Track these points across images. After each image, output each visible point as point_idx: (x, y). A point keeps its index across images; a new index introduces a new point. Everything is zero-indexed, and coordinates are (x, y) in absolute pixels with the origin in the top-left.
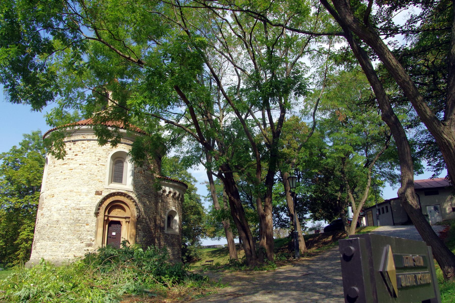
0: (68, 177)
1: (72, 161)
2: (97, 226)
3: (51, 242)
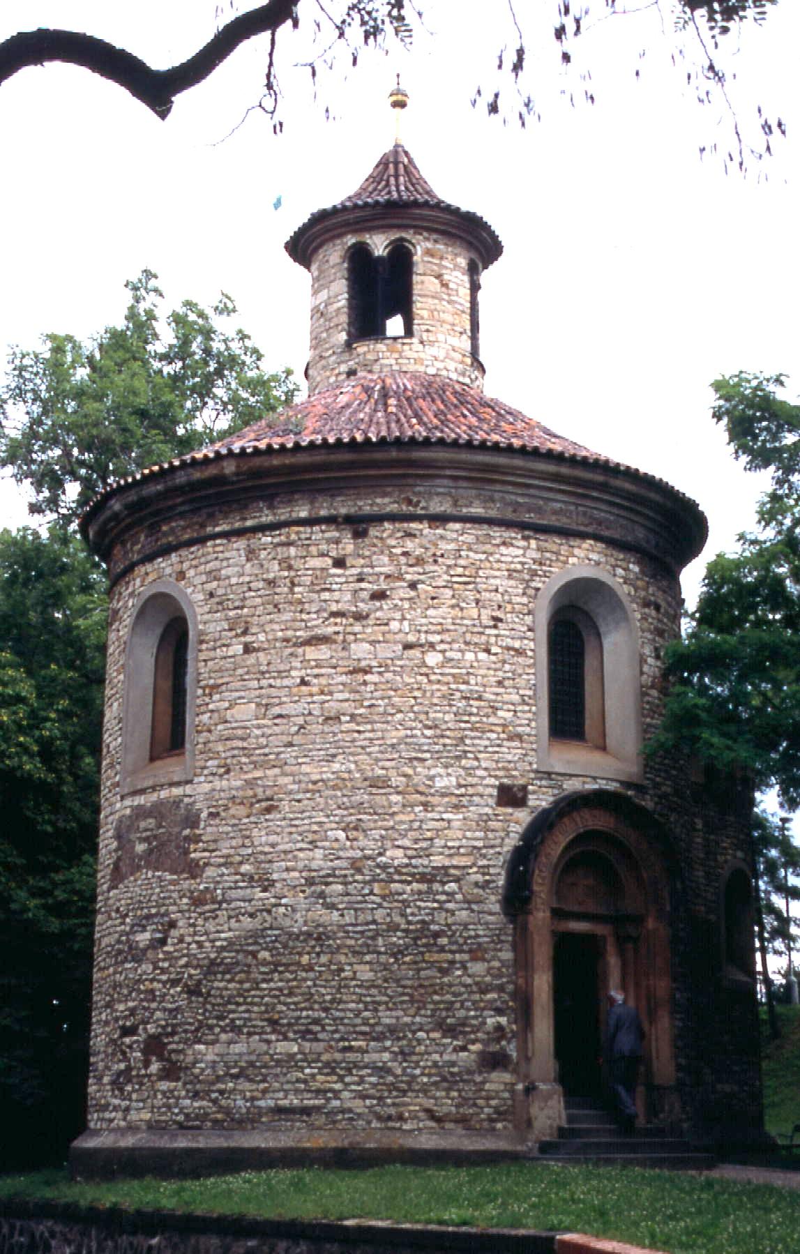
1: (357, 628)
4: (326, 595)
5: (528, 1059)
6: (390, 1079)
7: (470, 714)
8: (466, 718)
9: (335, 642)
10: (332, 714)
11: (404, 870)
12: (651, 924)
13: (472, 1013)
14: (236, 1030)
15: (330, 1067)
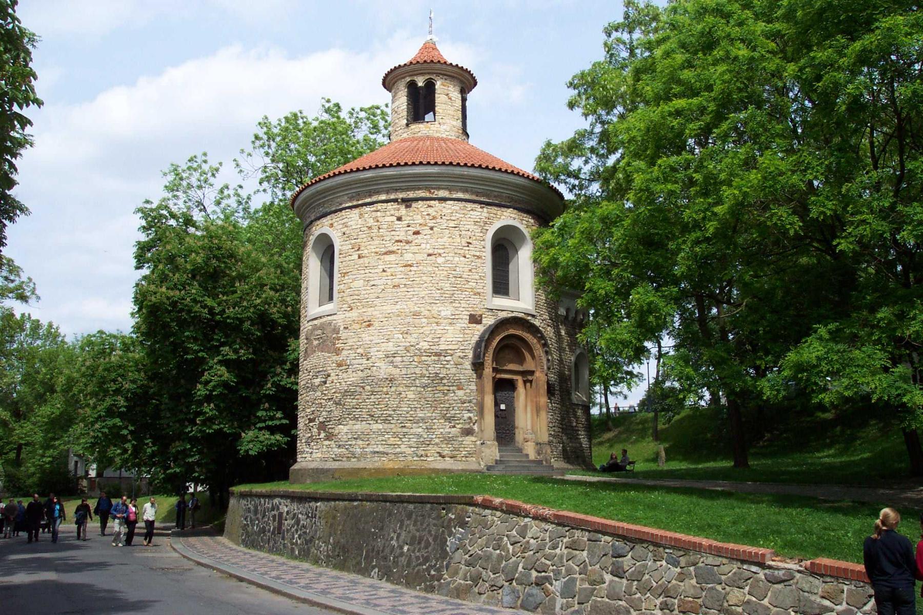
1: (407, 247)
2: (481, 390)
3: (381, 427)
4: (393, 233)
5: (482, 431)
6: (422, 440)
12: (537, 374)
14: (356, 419)
15: (395, 435)
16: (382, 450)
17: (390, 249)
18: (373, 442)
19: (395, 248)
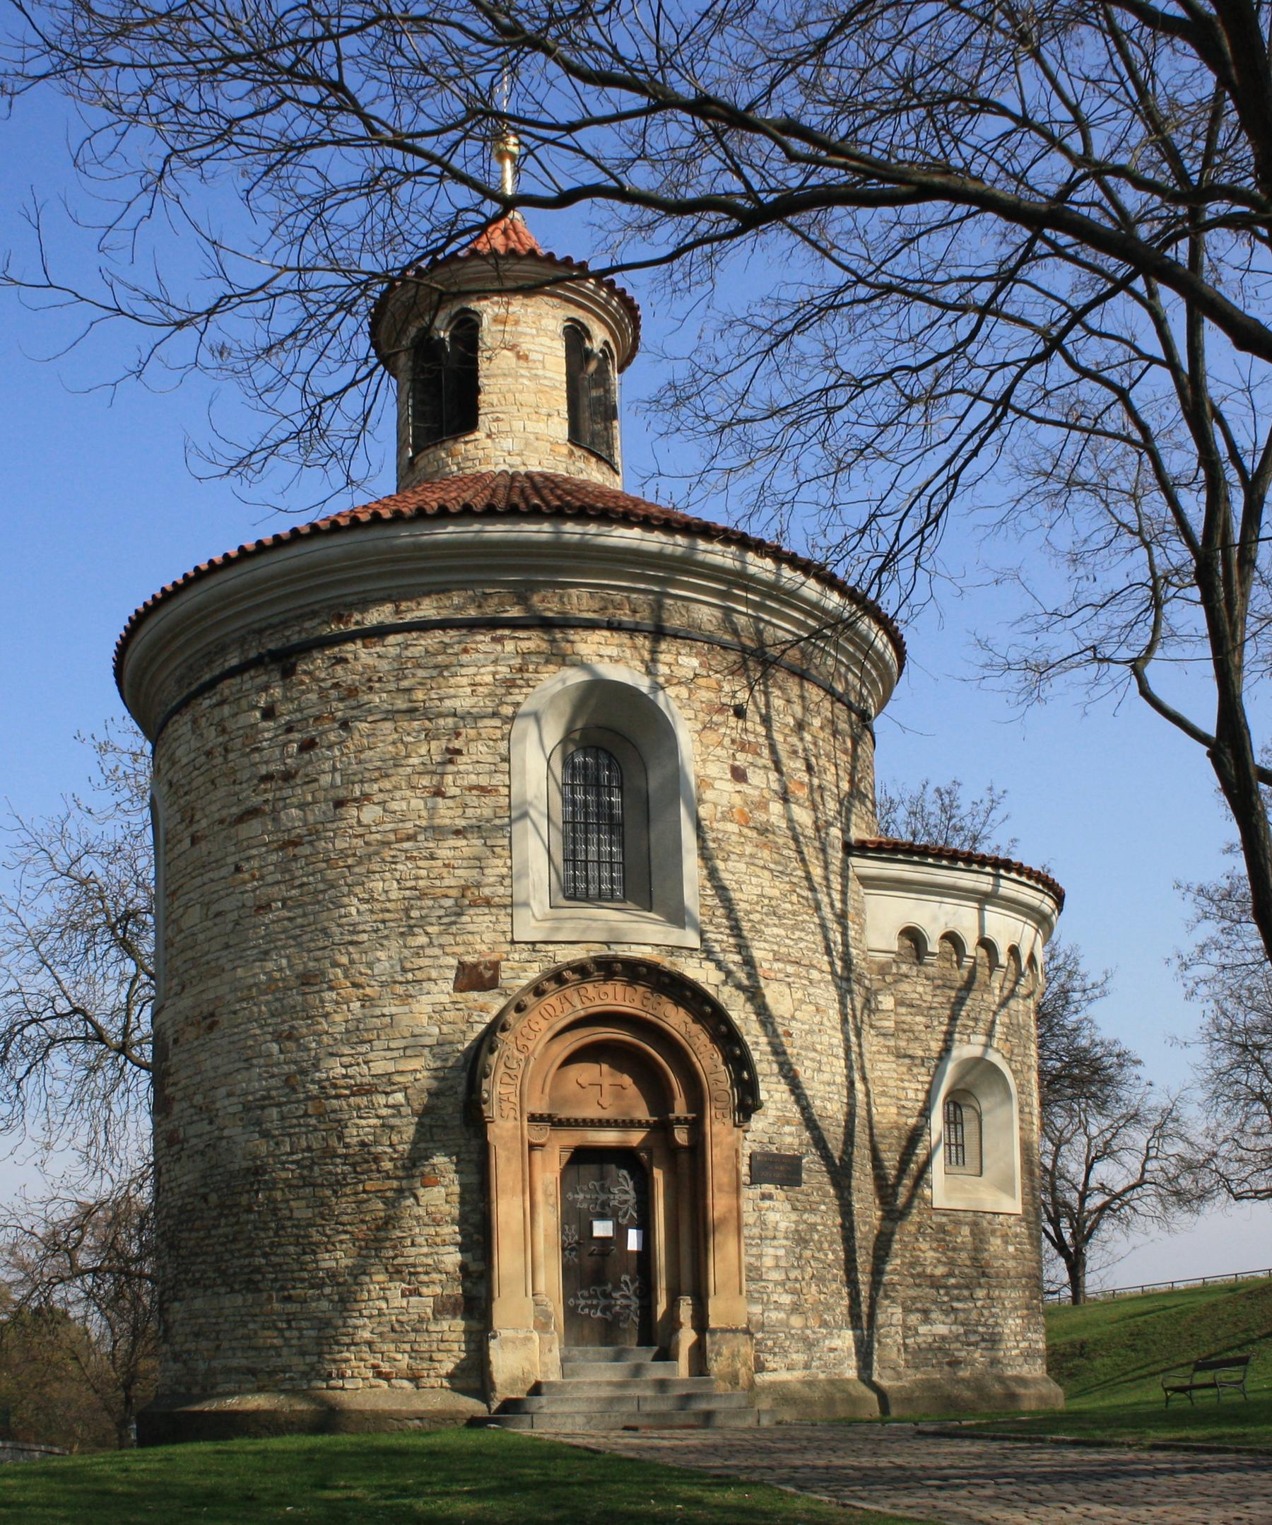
0: (282, 891)
3: (239, 1300)
7: (417, 878)
8: (413, 883)
9: (264, 813)
10: (263, 903)
11: (341, 1082)
13: (425, 1250)
16: (244, 1362)
17: (249, 804)
18: (225, 1344)
19: (256, 800)
